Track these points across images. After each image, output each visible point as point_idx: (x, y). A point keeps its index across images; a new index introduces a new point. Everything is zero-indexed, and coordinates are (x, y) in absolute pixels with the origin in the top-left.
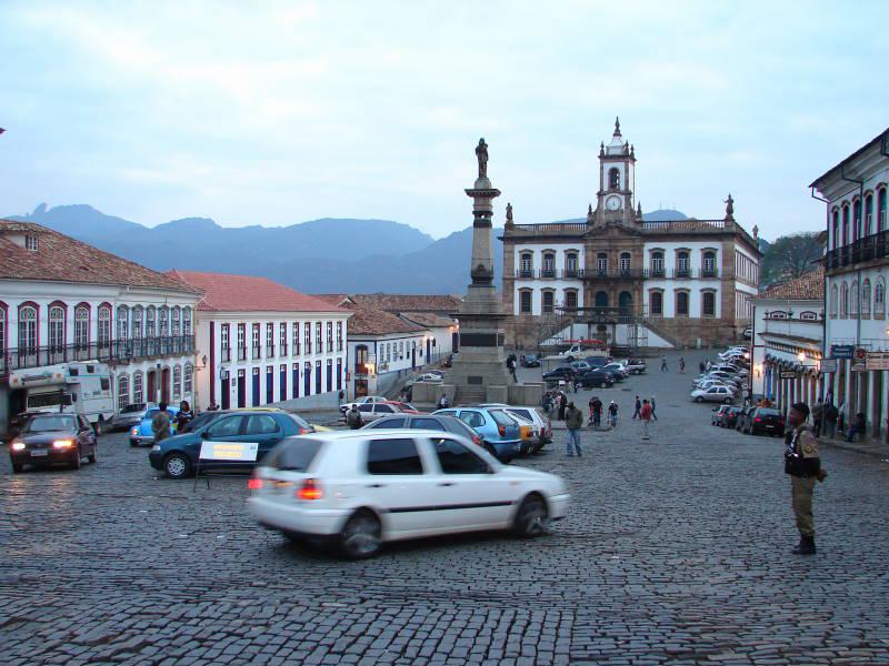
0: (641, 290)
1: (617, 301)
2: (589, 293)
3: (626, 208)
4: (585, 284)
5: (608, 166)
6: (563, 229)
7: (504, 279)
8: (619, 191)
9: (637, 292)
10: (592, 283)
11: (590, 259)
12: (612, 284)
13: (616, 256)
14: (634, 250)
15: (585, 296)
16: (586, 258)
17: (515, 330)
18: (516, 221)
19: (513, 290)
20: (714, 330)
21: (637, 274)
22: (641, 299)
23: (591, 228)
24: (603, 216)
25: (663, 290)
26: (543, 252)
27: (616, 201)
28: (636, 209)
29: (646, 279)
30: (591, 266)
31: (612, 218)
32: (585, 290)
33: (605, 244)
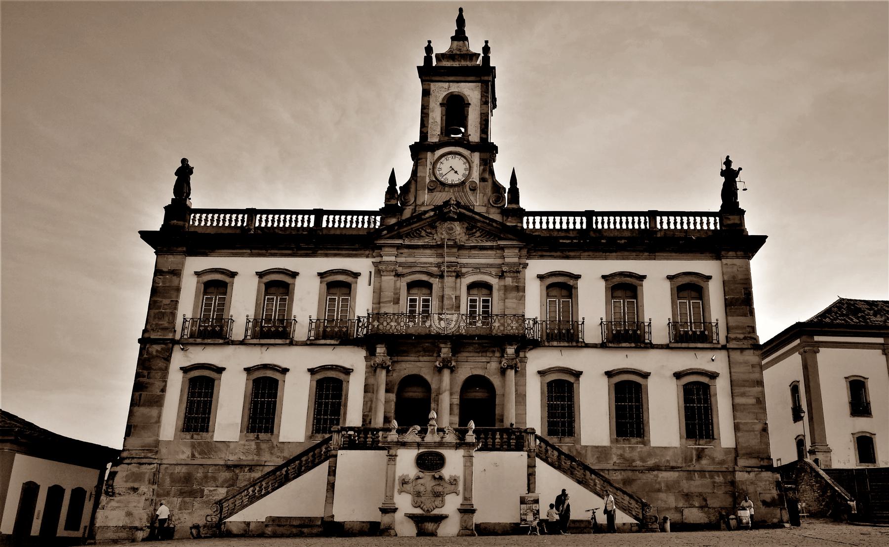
0: (520, 373)
1: (456, 401)
2: (382, 375)
3: (483, 180)
4: (371, 353)
5: (441, 90)
6: (318, 221)
7: (140, 341)
8: (464, 143)
9: (511, 373)
10: (390, 353)
11: (388, 294)
12: (445, 351)
13: (455, 288)
14: (501, 276)
15: (368, 389)
16: (378, 294)
17: (154, 481)
18: (196, 201)
19: (165, 371)
20: (719, 479)
21: (513, 327)
22: (521, 398)
23: (393, 221)
24: (425, 197)
25: (578, 374)
26: (260, 275)
27: (458, 164)
28: (507, 185)
29: (535, 344)
30: (389, 309)
31: (440, 198)
32: (372, 370)
33: (428, 259)
